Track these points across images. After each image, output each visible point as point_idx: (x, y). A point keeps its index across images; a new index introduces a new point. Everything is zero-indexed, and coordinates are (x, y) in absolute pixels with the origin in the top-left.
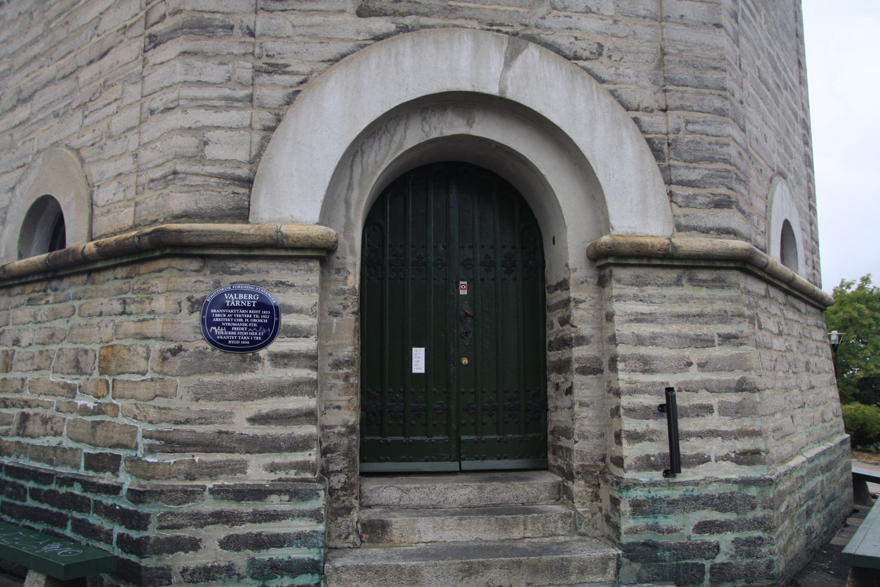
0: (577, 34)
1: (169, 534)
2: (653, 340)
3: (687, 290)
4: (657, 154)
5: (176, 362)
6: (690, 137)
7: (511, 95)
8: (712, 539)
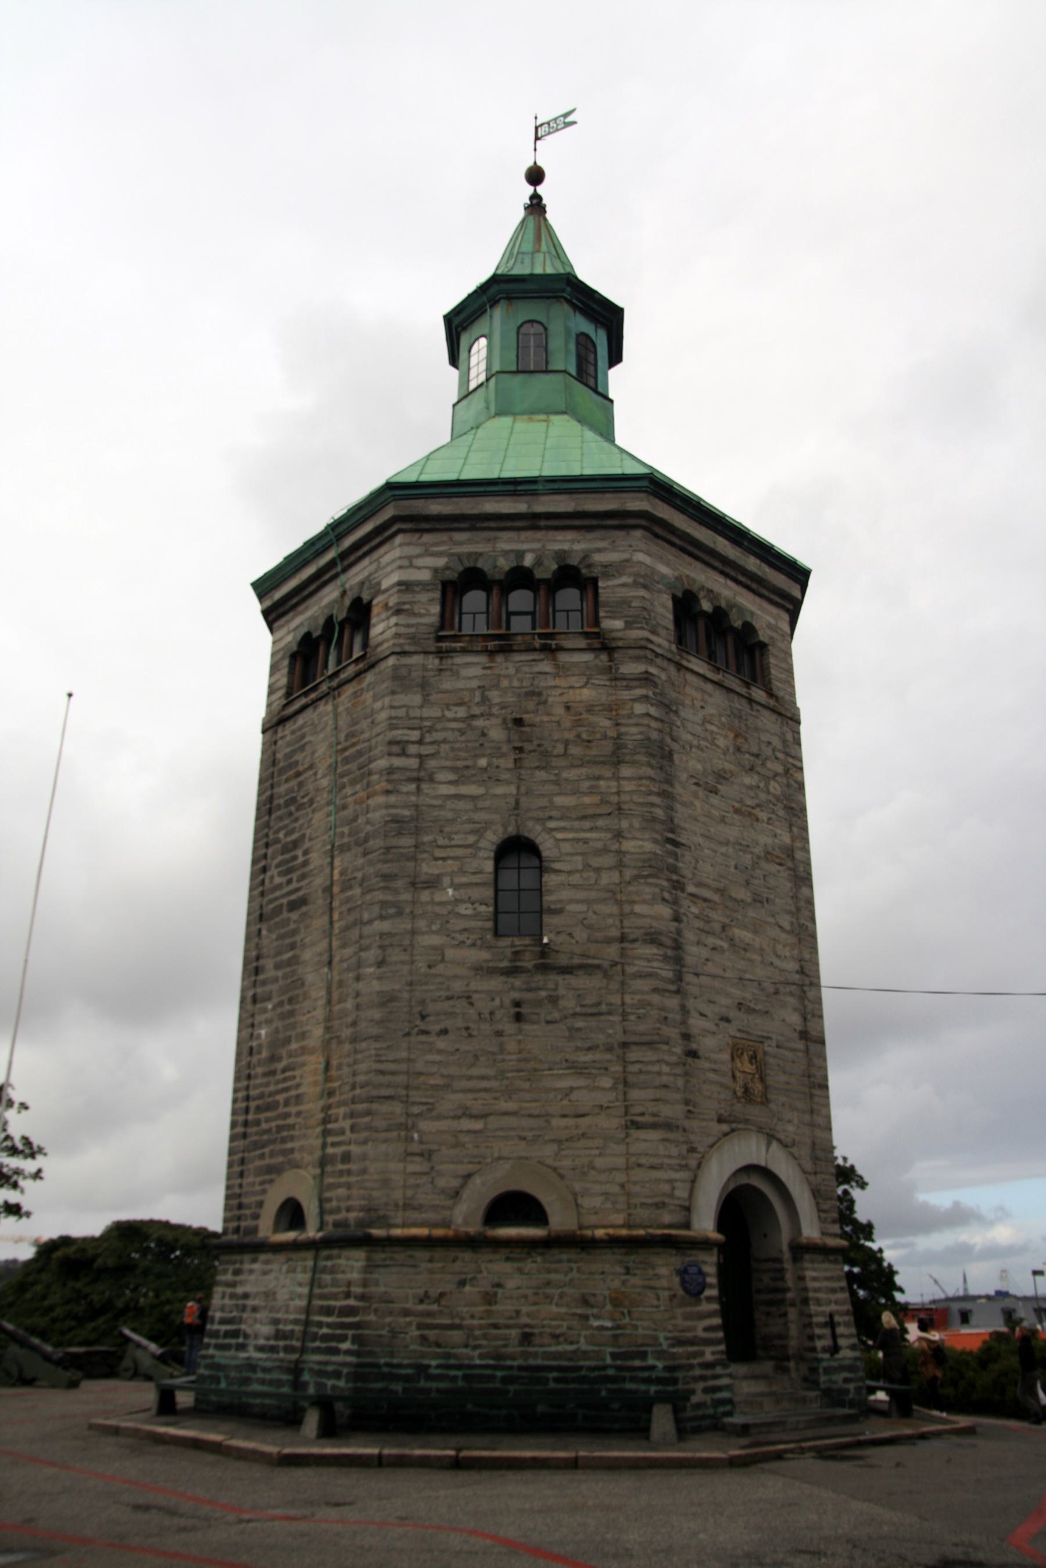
3: (827, 1265)
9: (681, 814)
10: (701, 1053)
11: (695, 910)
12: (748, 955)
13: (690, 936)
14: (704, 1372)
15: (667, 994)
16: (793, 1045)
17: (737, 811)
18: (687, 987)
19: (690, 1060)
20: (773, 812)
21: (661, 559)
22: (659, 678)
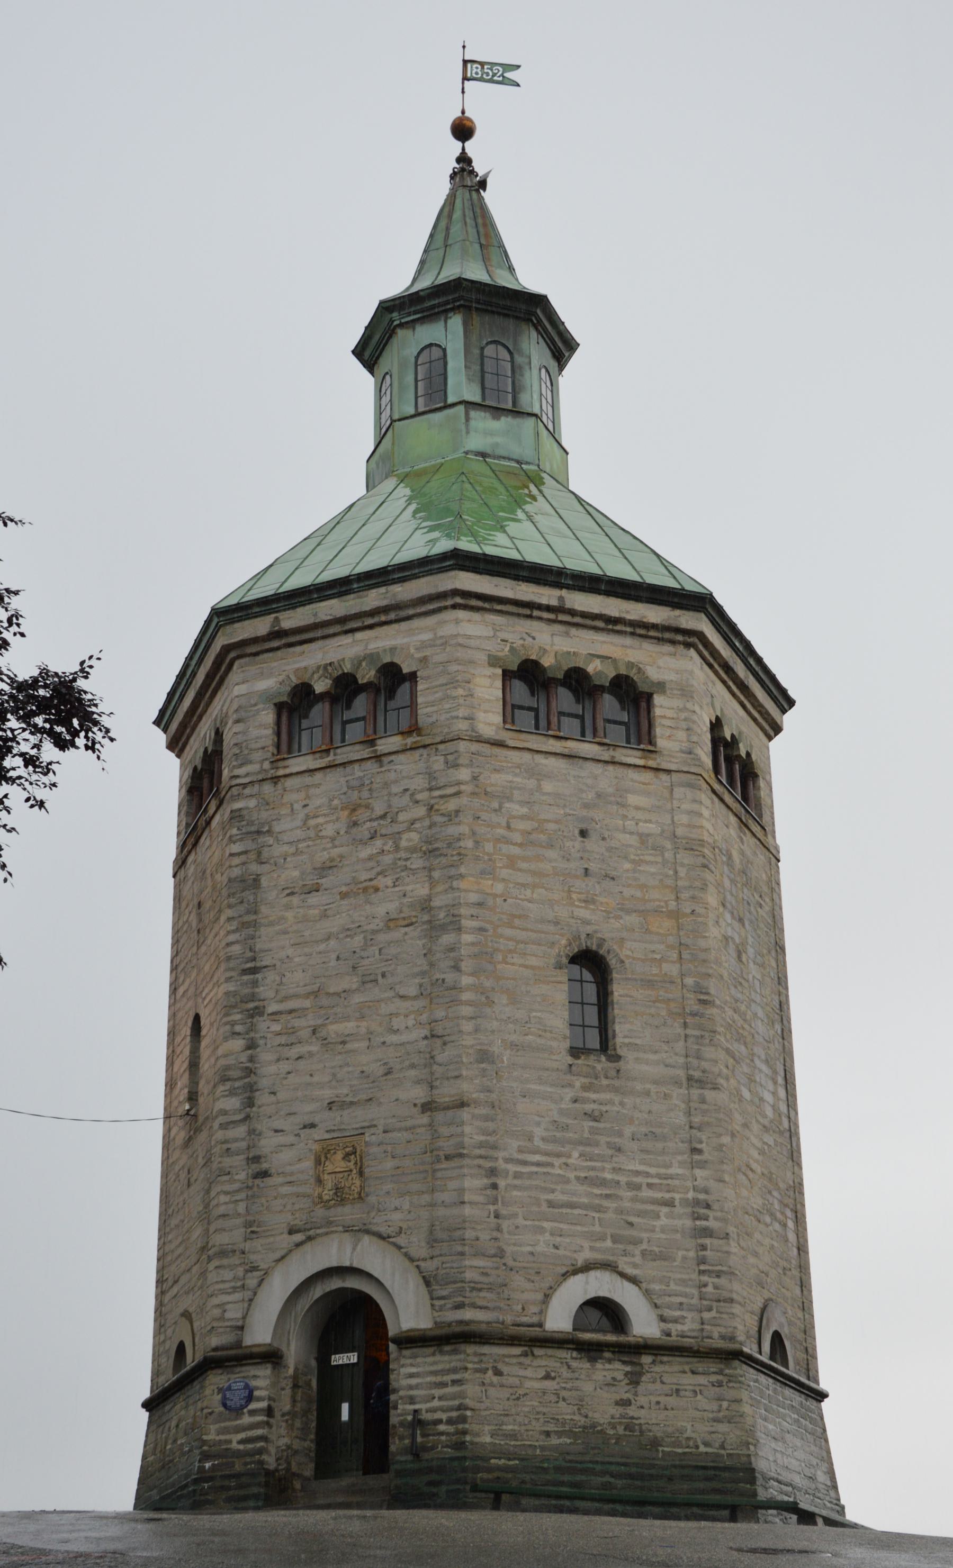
0: (389, 1223)
1: (202, 1498)
2: (417, 1387)
3: (438, 1358)
4: (427, 1283)
5: (211, 1418)
6: (444, 1271)
7: (355, 1265)
8: (435, 1490)
9: (266, 938)
10: (273, 1171)
11: (276, 1027)
12: (349, 1046)
13: (265, 1056)
14: (226, 1483)
15: (232, 1126)
16: (409, 1123)
17: (344, 896)
18: (261, 1109)
19: (257, 1181)
20: (406, 868)
21: (262, 676)
22: (247, 808)
